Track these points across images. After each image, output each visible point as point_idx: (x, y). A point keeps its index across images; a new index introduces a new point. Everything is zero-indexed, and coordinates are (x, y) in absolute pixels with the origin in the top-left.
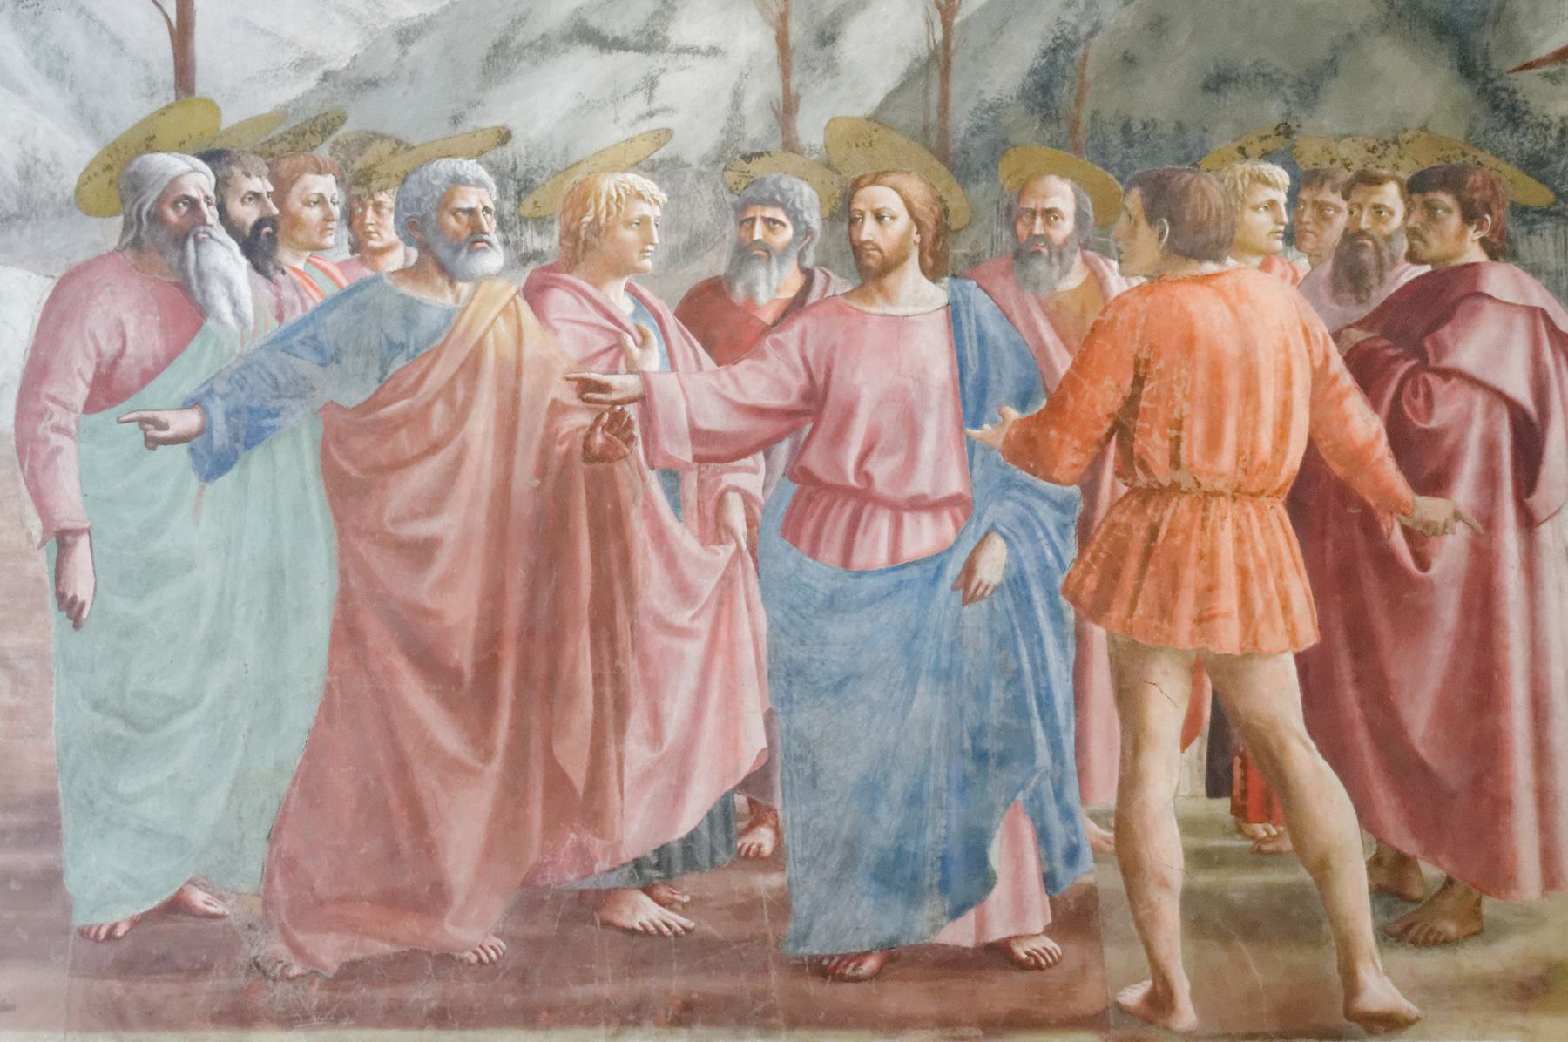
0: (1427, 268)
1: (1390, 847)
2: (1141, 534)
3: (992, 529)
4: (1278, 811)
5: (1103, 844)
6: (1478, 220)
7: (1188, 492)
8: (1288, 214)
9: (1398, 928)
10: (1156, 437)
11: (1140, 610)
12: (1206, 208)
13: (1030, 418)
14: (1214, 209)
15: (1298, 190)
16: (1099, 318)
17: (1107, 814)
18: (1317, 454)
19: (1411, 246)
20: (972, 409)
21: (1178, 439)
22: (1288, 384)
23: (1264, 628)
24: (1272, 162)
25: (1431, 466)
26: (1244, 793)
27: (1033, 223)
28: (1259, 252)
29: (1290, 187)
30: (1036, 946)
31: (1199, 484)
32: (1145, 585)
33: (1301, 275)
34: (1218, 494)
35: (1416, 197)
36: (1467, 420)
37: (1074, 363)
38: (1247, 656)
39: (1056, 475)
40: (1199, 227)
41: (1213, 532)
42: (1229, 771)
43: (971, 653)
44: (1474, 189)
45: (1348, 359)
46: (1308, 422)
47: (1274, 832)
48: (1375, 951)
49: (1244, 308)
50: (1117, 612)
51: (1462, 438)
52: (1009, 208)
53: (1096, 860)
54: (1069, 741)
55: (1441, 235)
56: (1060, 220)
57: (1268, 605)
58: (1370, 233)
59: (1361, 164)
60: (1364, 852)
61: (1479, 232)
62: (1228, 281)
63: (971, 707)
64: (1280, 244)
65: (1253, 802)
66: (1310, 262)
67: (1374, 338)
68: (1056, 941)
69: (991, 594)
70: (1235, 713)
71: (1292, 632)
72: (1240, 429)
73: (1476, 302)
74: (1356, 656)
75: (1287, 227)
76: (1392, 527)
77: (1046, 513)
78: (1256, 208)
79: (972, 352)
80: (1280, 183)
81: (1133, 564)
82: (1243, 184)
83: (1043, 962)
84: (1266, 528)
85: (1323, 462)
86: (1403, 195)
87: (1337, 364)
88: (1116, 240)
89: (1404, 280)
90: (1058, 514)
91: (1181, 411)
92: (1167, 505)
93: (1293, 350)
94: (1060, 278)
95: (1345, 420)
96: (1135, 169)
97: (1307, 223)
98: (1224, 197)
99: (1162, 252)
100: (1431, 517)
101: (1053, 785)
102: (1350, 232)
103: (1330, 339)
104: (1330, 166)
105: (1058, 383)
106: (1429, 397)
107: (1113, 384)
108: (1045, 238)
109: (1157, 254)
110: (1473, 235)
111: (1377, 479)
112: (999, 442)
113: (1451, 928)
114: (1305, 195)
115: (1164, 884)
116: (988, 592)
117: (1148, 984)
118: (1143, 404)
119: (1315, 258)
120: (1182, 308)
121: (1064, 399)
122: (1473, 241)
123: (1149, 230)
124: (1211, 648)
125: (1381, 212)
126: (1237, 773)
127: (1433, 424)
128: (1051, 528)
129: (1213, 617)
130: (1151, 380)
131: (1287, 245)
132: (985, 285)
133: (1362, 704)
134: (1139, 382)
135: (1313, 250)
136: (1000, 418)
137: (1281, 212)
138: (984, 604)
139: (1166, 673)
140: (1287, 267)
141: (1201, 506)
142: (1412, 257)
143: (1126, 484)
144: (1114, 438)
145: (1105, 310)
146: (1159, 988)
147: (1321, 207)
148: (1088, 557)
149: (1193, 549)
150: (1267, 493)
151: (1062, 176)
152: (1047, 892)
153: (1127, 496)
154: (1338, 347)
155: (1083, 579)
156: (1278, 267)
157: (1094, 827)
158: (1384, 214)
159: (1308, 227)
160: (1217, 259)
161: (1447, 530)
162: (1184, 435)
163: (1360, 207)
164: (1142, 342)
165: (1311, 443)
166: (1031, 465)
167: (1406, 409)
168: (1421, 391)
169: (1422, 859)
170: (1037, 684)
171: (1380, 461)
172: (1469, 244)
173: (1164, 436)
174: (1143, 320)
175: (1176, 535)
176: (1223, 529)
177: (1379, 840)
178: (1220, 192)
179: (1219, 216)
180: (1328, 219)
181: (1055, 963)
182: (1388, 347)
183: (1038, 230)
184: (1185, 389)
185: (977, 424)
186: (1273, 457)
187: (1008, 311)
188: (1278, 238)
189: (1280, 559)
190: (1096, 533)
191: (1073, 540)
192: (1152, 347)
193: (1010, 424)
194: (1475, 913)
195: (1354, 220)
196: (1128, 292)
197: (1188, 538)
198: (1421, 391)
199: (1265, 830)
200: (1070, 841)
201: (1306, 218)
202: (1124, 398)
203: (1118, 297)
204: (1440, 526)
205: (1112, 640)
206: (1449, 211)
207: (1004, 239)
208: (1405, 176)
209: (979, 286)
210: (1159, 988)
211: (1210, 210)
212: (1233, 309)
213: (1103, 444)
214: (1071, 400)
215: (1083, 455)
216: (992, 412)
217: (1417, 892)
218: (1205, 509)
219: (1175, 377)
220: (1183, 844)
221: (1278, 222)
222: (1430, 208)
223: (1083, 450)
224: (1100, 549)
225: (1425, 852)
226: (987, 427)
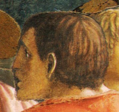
82: (115, 25)
160: (94, 86)
178: (98, 32)
179: (96, 51)
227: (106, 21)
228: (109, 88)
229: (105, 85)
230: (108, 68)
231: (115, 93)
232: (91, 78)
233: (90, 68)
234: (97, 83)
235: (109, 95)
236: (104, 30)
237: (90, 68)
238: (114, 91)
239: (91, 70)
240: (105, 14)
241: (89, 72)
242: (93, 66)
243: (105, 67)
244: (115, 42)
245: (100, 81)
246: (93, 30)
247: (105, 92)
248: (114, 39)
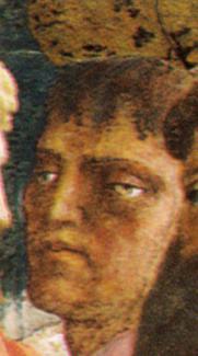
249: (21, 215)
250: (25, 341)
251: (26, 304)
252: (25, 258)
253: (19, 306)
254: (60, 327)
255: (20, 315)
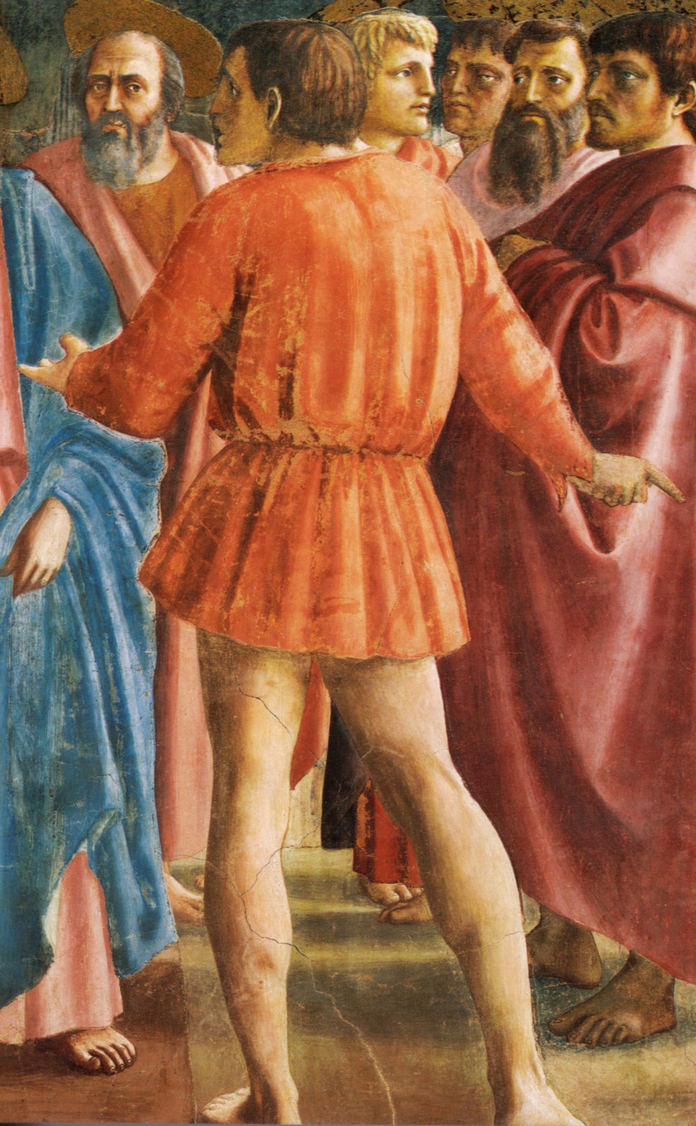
0: (615, 154)
1: (558, 915)
2: (243, 501)
3: (52, 493)
4: (414, 867)
5: (190, 910)
6: (682, 88)
7: (303, 447)
8: (435, 83)
9: (565, 1022)
10: (263, 378)
11: (239, 602)
12: (329, 73)
13: (102, 350)
14: (339, 71)
15: (449, 49)
16: (191, 220)
17: (196, 871)
18: (469, 398)
19: (593, 124)
20: (26, 341)
21: (290, 380)
22: (431, 308)
23: (398, 624)
24: (416, 13)
25: (617, 411)
26: (371, 844)
27: (107, 95)
28: (395, 132)
29: (437, 45)
30: (103, 1044)
31: (316, 437)
32: (247, 567)
33: (451, 164)
34: (343, 450)
35: (601, 59)
36: (665, 354)
37: (158, 280)
38: (375, 662)
39: (133, 423)
40: (319, 98)
41: (334, 498)
42: (352, 812)
43: (23, 657)
44: (675, 47)
45: (510, 278)
46: (457, 358)
47: (408, 894)
48: (536, 1055)
49: (379, 208)
50: (209, 605)
51: (655, 379)
52: (76, 76)
53: (181, 933)
54: (145, 771)
55: (632, 109)
56: (141, 91)
57: (404, 593)
58: (541, 106)
59: (531, 14)
60: (524, 923)
61: (681, 105)
62: (356, 170)
63: (23, 730)
64: (423, 123)
65: (382, 857)
66: (462, 146)
67: (543, 247)
68: (128, 1037)
69: (49, 582)
70: (361, 736)
71: (435, 635)
72: (370, 364)
73: (676, 199)
74: (517, 662)
75: (433, 99)
76: (566, 494)
77: (119, 473)
78: (393, 73)
79: (28, 273)
80: (424, 39)
81: (231, 539)
82: (377, 41)
83: (111, 1063)
84: (402, 495)
85: (477, 410)
86: (583, 55)
87: (495, 282)
88: (213, 116)
89: (584, 170)
90: (135, 477)
91: (294, 341)
92: (276, 464)
93: (439, 265)
94: (141, 167)
95: (506, 355)
96: (238, 21)
97: (460, 93)
98: (353, 59)
99: (273, 132)
100: (615, 481)
101: (126, 831)
102: (514, 105)
103: (487, 250)
104: (491, 16)
105: (137, 306)
106: (615, 326)
107: (208, 307)
108: (123, 115)
109: (265, 134)
110: (673, 108)
111: (546, 432)
112: (61, 382)
113: (635, 1022)
114: (456, 56)
115: (266, 963)
116: (46, 578)
117: (245, 1092)
118: (246, 332)
119: (466, 138)
120: (297, 206)
121: (145, 326)
122: (674, 117)
123: (256, 103)
124: (331, 650)
125: (555, 79)
126: (362, 816)
127: (621, 359)
128: (127, 493)
129: (332, 610)
130: (256, 302)
131: (433, 123)
132: (44, 175)
133: (524, 724)
134: (240, 304)
135: (466, 130)
136: (63, 351)
137: (425, 78)
138: (40, 593)
139: (271, 684)
140: (432, 153)
141: (319, 466)
142: (595, 140)
143: (223, 437)
144: (209, 375)
145: (199, 209)
146: (259, 1099)
147: (477, 72)
148: (173, 532)
149: (308, 522)
150: (403, 451)
151: (146, 32)
152: (117, 973)
153: (223, 452)
154: (497, 258)
155: (167, 559)
156: (420, 155)
157: (178, 888)
158: (559, 81)
159: (460, 99)
160: (343, 141)
161: (635, 498)
162: (297, 373)
163: (528, 72)
164: (245, 251)
165: (462, 383)
166: (103, 412)
167: (584, 339)
168: (605, 315)
169: (598, 932)
170: (107, 698)
171: (550, 407)
172: (669, 120)
173: (272, 374)
174: (246, 221)
175: (287, 504)
176: (346, 497)
177: (542, 908)
178: (349, 53)
179: (346, 83)
180: (488, 90)
181: (126, 1065)
182: (561, 260)
183: (114, 104)
184: (299, 314)
185: (34, 359)
186: (412, 403)
187: (73, 210)
188: (421, 114)
189: (419, 535)
190: (184, 500)
191: (155, 513)
192: (257, 259)
193: (76, 357)
194: (667, 1003)
195: (519, 89)
196: (227, 185)
197: (300, 510)
198: (605, 315)
199: (397, 891)
200: (146, 906)
201: (457, 87)
202: (222, 325)
203: (215, 193)
204: (628, 493)
205: (203, 640)
206: (643, 76)
207: (70, 117)
208: (585, 29)
209: (37, 178)
210: (259, 1099)
211: (334, 76)
212: (363, 209)
213: (194, 385)
214: (153, 329)
215: (168, 399)
216: (53, 343)
217: (592, 975)
218: (324, 470)
219: (287, 297)
220: (292, 910)
221: (420, 92)
222: (619, 73)
223: (168, 392)
224: (188, 520)
225: (601, 922)
226: (45, 362)
227: (361, 33)
228: (368, 144)
229: (362, 139)
230: (366, 111)
231: (378, 152)
232: (338, 127)
233: (337, 112)
234: (348, 137)
235: (368, 156)
236: (359, 49)
237: (337, 112)
238: (376, 148)
239: (338, 115)
240: (360, 23)
241: (335, 117)
242: (341, 108)
243: (361, 110)
244: (376, 68)
245: (354, 132)
246: (341, 50)
247: (361, 151)
248: (375, 64)
249: (440, 89)
250: (442, 146)
251: (443, 130)
252: (442, 109)
253: (440, 130)
254: (458, 140)
255: (440, 135)
